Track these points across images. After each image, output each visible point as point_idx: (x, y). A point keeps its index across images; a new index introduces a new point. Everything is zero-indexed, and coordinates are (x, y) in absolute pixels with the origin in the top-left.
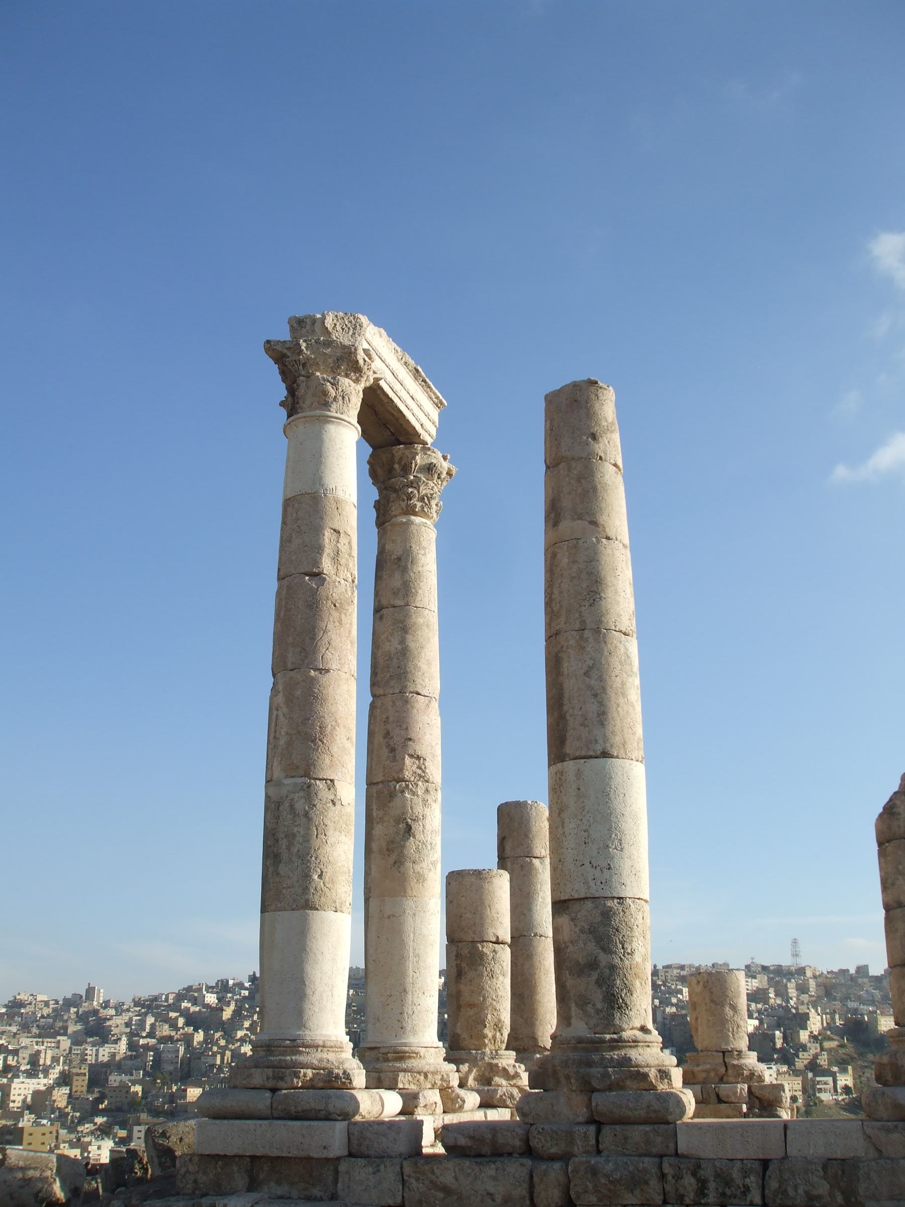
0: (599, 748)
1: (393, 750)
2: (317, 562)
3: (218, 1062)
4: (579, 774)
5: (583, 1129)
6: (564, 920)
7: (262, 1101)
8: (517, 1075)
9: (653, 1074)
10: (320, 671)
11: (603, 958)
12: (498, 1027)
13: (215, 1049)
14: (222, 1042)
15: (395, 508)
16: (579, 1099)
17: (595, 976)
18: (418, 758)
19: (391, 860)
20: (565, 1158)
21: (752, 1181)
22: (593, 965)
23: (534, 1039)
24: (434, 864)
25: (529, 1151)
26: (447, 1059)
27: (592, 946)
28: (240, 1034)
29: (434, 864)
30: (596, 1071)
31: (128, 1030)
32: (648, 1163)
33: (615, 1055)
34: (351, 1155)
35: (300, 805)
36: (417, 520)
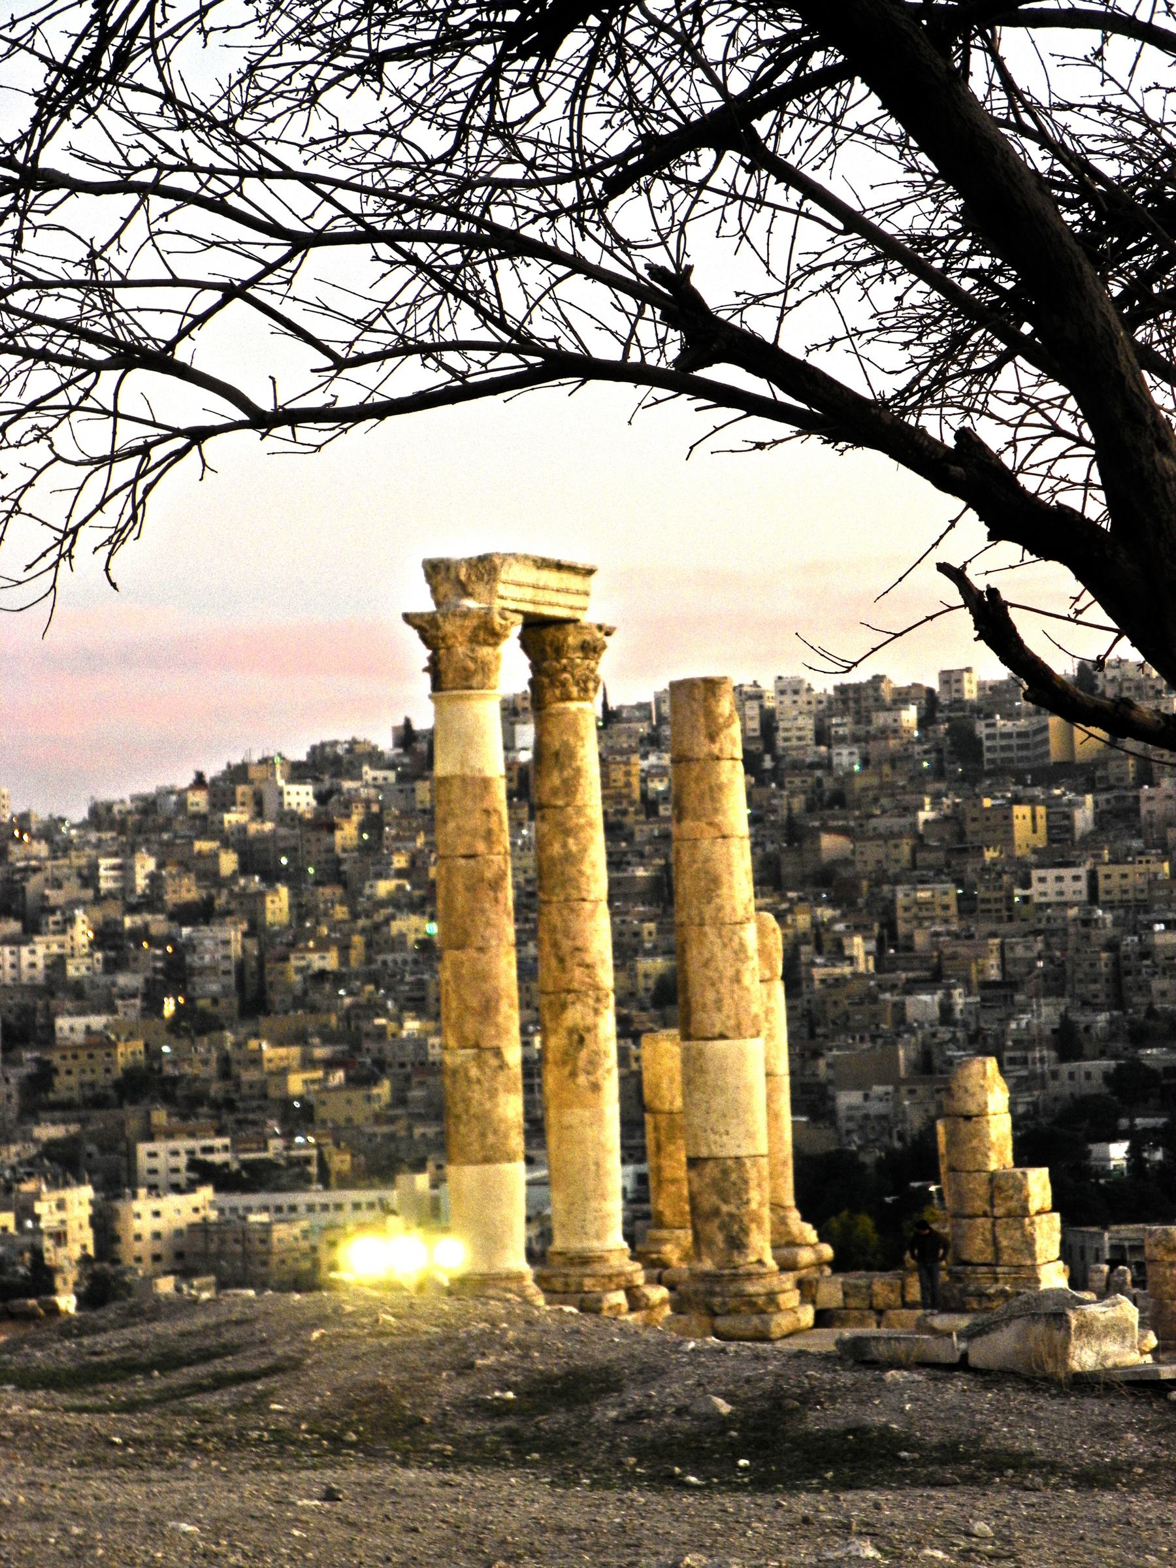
0: (717, 1030)
1: (561, 960)
4: (701, 1053)
10: (481, 950)
11: (725, 1208)
14: (341, 912)
17: (717, 1222)
18: (588, 966)
19: (567, 1071)
22: (716, 1212)
24: (608, 1071)
26: (632, 1258)
27: (715, 1199)
29: (608, 1071)
30: (717, 1300)
31: (89, 893)
33: (733, 1288)
36: (573, 706)
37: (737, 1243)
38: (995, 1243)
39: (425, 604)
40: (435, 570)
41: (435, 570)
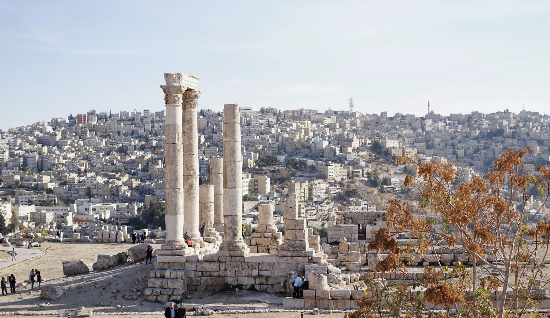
2: (175, 141)
3: (56, 162)
5: (228, 258)
6: (226, 219)
7: (169, 252)
8: (215, 234)
9: (241, 248)
11: (233, 227)
12: (211, 223)
13: (54, 156)
14: (58, 152)
15: (188, 106)
16: (228, 252)
20: (226, 262)
21: (257, 266)
23: (219, 221)
25: (219, 261)
28: (66, 148)
32: (240, 263)
34: (186, 262)
35: (173, 194)
36: (192, 110)
37: (235, 235)
38: (296, 235)
39: (165, 84)
40: (167, 75)
41: (167, 75)
